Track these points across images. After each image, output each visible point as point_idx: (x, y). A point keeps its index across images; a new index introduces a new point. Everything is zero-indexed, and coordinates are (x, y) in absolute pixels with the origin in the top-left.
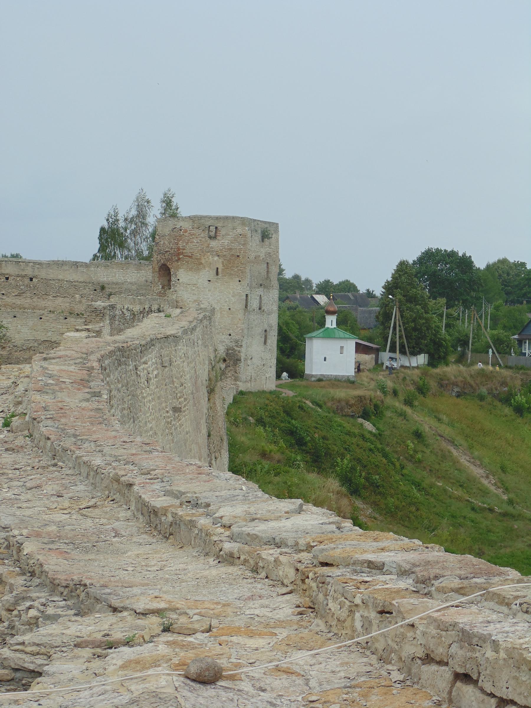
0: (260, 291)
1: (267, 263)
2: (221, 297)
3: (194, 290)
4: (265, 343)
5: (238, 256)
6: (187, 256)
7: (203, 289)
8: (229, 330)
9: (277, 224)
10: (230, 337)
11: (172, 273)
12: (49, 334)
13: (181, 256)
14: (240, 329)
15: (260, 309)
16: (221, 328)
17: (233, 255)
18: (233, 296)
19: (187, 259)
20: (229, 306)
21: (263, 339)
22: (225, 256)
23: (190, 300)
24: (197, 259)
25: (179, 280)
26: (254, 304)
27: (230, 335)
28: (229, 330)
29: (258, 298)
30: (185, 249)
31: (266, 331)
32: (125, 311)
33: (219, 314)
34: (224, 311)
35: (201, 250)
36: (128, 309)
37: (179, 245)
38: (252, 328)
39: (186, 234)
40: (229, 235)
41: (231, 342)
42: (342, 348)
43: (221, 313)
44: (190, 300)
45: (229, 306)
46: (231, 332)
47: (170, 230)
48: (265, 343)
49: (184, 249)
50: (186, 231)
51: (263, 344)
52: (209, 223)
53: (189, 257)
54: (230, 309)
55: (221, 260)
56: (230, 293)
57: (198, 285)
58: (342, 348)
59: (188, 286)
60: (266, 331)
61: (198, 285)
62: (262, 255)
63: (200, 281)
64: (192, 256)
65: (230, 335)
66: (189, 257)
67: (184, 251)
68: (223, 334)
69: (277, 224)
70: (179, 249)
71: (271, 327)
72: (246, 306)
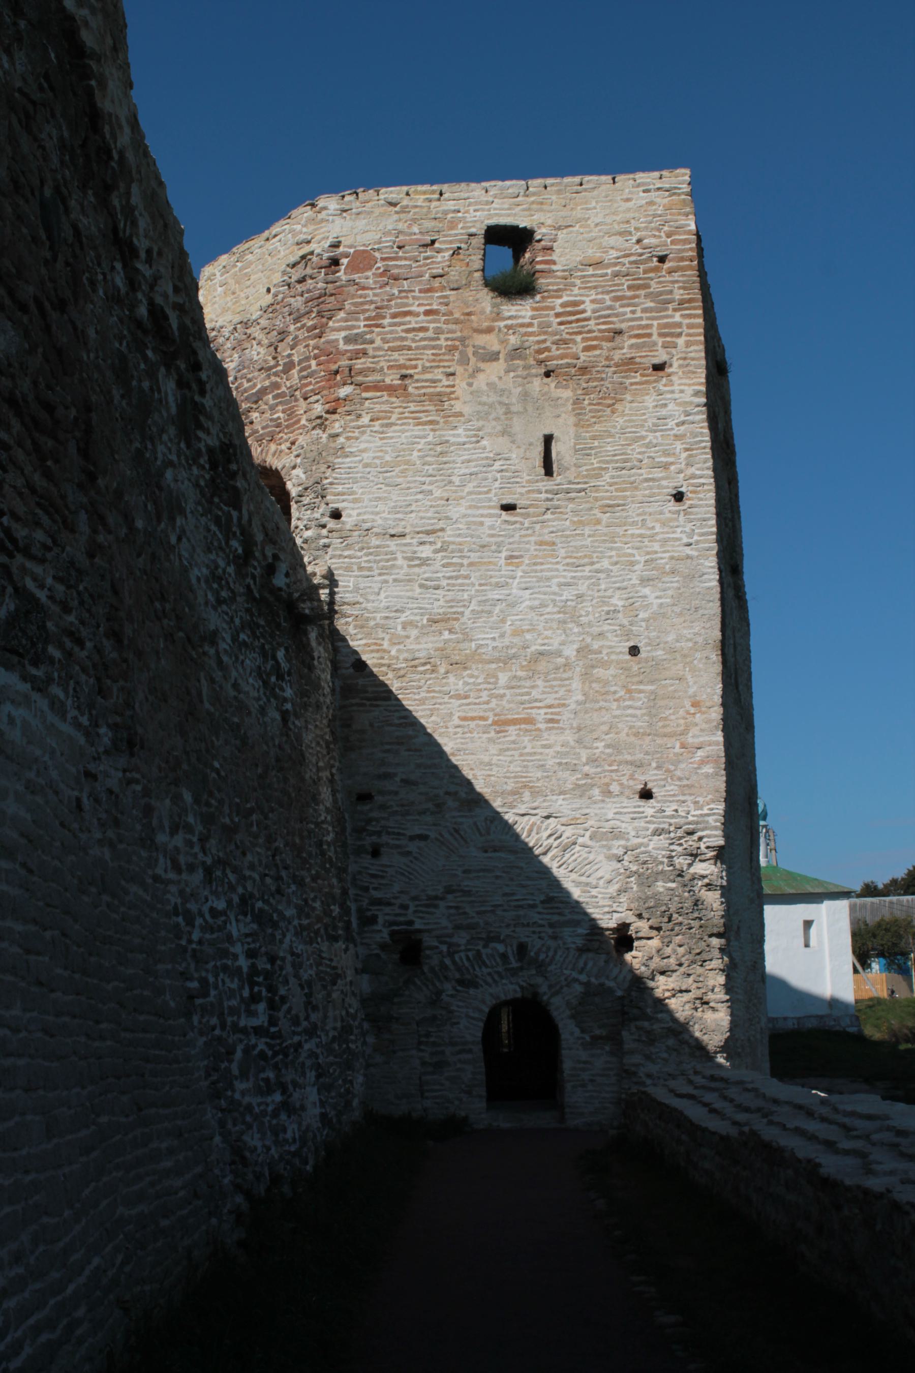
2: (583, 588)
3: (424, 562)
5: (659, 367)
6: (376, 387)
7: (474, 557)
8: (640, 765)
10: (649, 808)
11: (294, 491)
13: (344, 392)
14: (703, 762)
16: (592, 761)
17: (629, 365)
18: (645, 581)
19: (380, 402)
20: (628, 635)
22: (584, 370)
23: (403, 618)
24: (439, 399)
25: (336, 515)
27: (646, 795)
28: (640, 765)
30: (365, 353)
33: (576, 684)
34: (605, 664)
35: (451, 349)
39: (369, 278)
41: (658, 832)
43: (586, 676)
44: (403, 618)
45: (628, 635)
46: (651, 777)
47: (277, 278)
50: (363, 260)
53: (391, 389)
54: (634, 651)
55: (567, 394)
56: (632, 564)
57: (449, 535)
59: (393, 544)
61: (449, 535)
63: (456, 511)
64: (405, 388)
65: (646, 795)
66: (391, 389)
67: (359, 364)
68: (607, 793)
70: (328, 353)
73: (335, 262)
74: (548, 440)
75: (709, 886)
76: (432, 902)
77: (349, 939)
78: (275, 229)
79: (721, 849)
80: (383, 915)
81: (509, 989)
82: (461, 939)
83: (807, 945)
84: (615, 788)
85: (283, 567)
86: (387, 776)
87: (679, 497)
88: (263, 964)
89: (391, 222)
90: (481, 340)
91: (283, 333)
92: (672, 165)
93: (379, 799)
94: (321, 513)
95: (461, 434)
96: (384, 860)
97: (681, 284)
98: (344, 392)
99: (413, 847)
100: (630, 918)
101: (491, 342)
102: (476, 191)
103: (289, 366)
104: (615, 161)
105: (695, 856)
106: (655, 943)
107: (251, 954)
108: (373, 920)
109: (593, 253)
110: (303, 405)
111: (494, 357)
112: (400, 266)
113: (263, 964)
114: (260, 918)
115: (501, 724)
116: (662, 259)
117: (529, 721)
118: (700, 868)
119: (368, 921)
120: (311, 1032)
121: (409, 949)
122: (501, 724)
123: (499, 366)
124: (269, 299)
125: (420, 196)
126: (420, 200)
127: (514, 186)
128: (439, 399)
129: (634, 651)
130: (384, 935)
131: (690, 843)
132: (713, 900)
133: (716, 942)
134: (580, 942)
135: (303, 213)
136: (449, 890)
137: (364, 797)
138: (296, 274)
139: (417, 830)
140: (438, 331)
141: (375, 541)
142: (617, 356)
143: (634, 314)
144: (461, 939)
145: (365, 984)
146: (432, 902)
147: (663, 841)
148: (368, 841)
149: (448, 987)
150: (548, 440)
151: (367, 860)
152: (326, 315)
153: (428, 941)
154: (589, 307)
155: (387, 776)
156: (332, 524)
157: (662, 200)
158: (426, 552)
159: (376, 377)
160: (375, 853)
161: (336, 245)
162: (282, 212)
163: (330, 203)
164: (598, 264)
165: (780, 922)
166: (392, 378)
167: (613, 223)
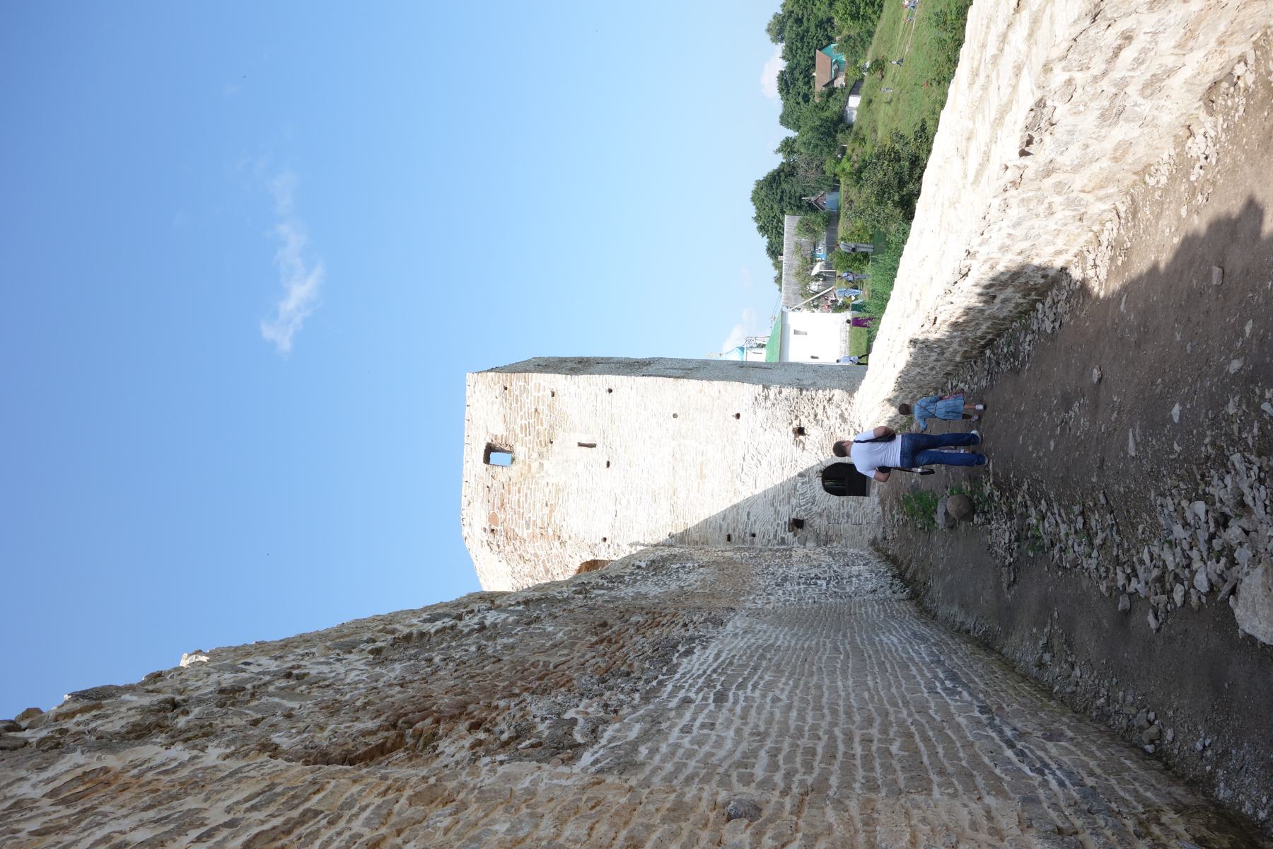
17: (551, 407)
19: (557, 515)
24: (558, 490)
25: (605, 539)
37: (525, 536)
39: (501, 516)
41: (755, 413)
42: (796, 332)
47: (496, 557)
49: (535, 523)
50: (493, 518)
53: (551, 511)
54: (675, 416)
58: (796, 332)
65: (738, 416)
66: (551, 511)
67: (539, 524)
74: (580, 445)
75: (780, 393)
76: (777, 512)
77: (791, 550)
78: (473, 557)
79: (764, 387)
80: (781, 534)
81: (818, 482)
82: (794, 501)
84: (734, 429)
85: (637, 563)
86: (721, 528)
87: (610, 391)
88: (802, 581)
89: (477, 505)
90: (533, 470)
91: (521, 557)
92: (465, 380)
93: (730, 532)
94: (603, 546)
96: (757, 532)
97: (517, 380)
98: (551, 533)
99: (752, 519)
100: (791, 428)
101: (535, 466)
102: (467, 468)
103: (536, 555)
104: (461, 405)
105: (766, 398)
106: (802, 418)
107: (799, 584)
108: (783, 539)
109: (500, 418)
110: (554, 550)
111: (541, 465)
112: (498, 502)
113: (802, 581)
114: (785, 579)
115: (702, 476)
117: (702, 464)
118: (772, 396)
119: (783, 541)
120: (830, 567)
121: (797, 524)
122: (702, 476)
123: (545, 462)
124: (504, 562)
125: (466, 490)
126: (468, 491)
127: (466, 449)
128: (558, 490)
129: (675, 416)
130: (790, 535)
131: (761, 399)
132: (786, 392)
133: (804, 392)
134: (800, 450)
135: (468, 544)
136: (773, 505)
137: (729, 538)
138: (494, 547)
139: (745, 516)
140: (528, 488)
142: (546, 412)
143: (529, 403)
144: (794, 501)
145: (811, 544)
146: (777, 512)
147: (759, 411)
148: (749, 538)
149: (815, 509)
150: (580, 445)
151: (756, 539)
152: (516, 537)
153: (794, 516)
154: (523, 422)
155: (721, 528)
156: (608, 542)
157: (480, 386)
158: (624, 501)
159: (546, 518)
160: (754, 535)
162: (466, 552)
163: (466, 531)
165: (798, 353)
166: (547, 510)
167: (485, 409)
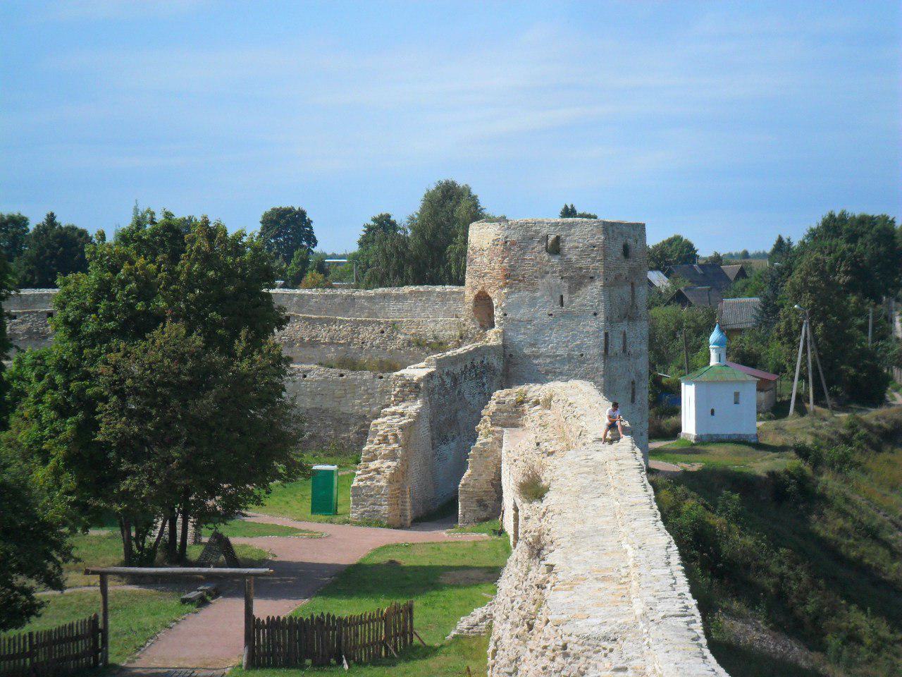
0: (623, 326)
1: (632, 284)
4: (633, 401)
5: (592, 278)
9: (644, 225)
11: (495, 305)
12: (318, 399)
15: (624, 351)
17: (584, 277)
21: (630, 396)
26: (616, 345)
29: (622, 336)
31: (633, 383)
32: (444, 377)
36: (448, 374)
38: (615, 381)
40: (577, 247)
42: (737, 395)
47: (491, 241)
48: (633, 401)
51: (629, 402)
52: (545, 231)
54: (582, 355)
58: (737, 395)
60: (633, 383)
62: (625, 272)
66: (520, 281)
69: (644, 225)
71: (639, 375)
72: (606, 349)
73: (506, 242)
83: (736, 402)
95: (538, 294)
109: (576, 244)
111: (548, 273)
116: (594, 247)
129: (582, 355)
141: (516, 323)
150: (562, 297)
161: (506, 237)
164: (577, 247)
166: (521, 278)
